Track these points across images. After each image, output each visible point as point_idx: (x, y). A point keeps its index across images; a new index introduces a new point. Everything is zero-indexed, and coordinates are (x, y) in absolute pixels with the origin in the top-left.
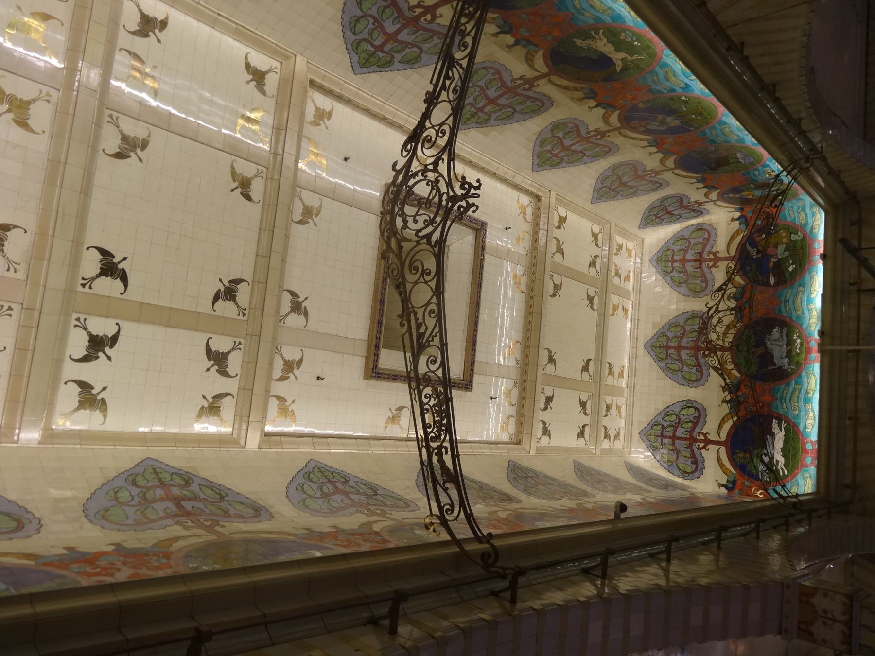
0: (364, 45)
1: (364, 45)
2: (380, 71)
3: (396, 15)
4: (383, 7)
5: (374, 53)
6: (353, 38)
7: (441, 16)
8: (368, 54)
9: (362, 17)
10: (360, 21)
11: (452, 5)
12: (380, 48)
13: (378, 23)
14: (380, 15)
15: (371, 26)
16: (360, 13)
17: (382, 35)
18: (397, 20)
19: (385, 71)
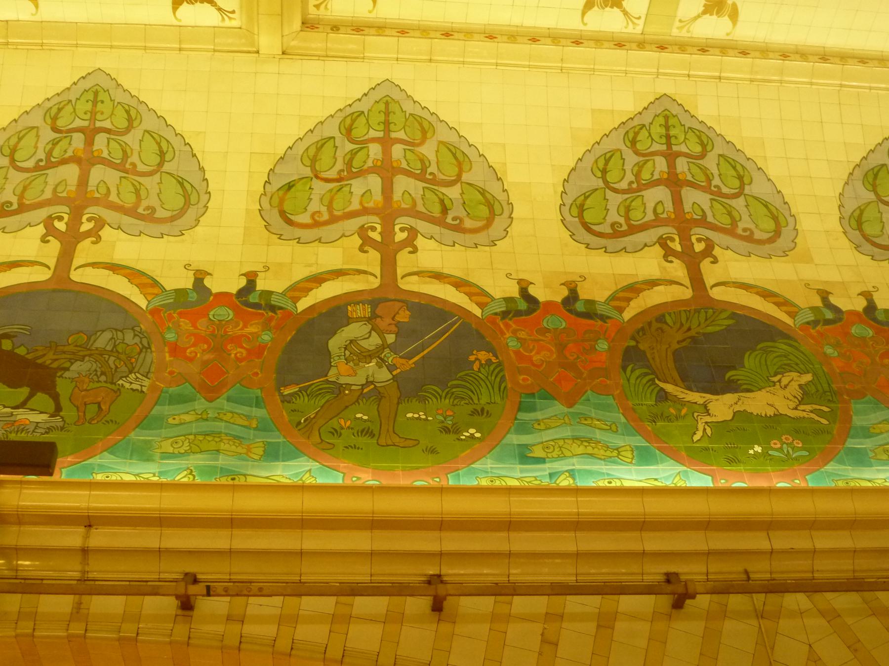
0: (121, 122)
1: (121, 122)
2: (58, 94)
3: (113, 198)
4: (143, 197)
5: (93, 119)
6: (144, 126)
7: (44, 240)
8: (102, 113)
9: (161, 164)
10: (159, 158)
11: (49, 268)
12: (90, 133)
13: (122, 167)
14: (137, 184)
15: (134, 159)
16: (167, 167)
17: (105, 154)
18: (103, 190)
19: (48, 99)
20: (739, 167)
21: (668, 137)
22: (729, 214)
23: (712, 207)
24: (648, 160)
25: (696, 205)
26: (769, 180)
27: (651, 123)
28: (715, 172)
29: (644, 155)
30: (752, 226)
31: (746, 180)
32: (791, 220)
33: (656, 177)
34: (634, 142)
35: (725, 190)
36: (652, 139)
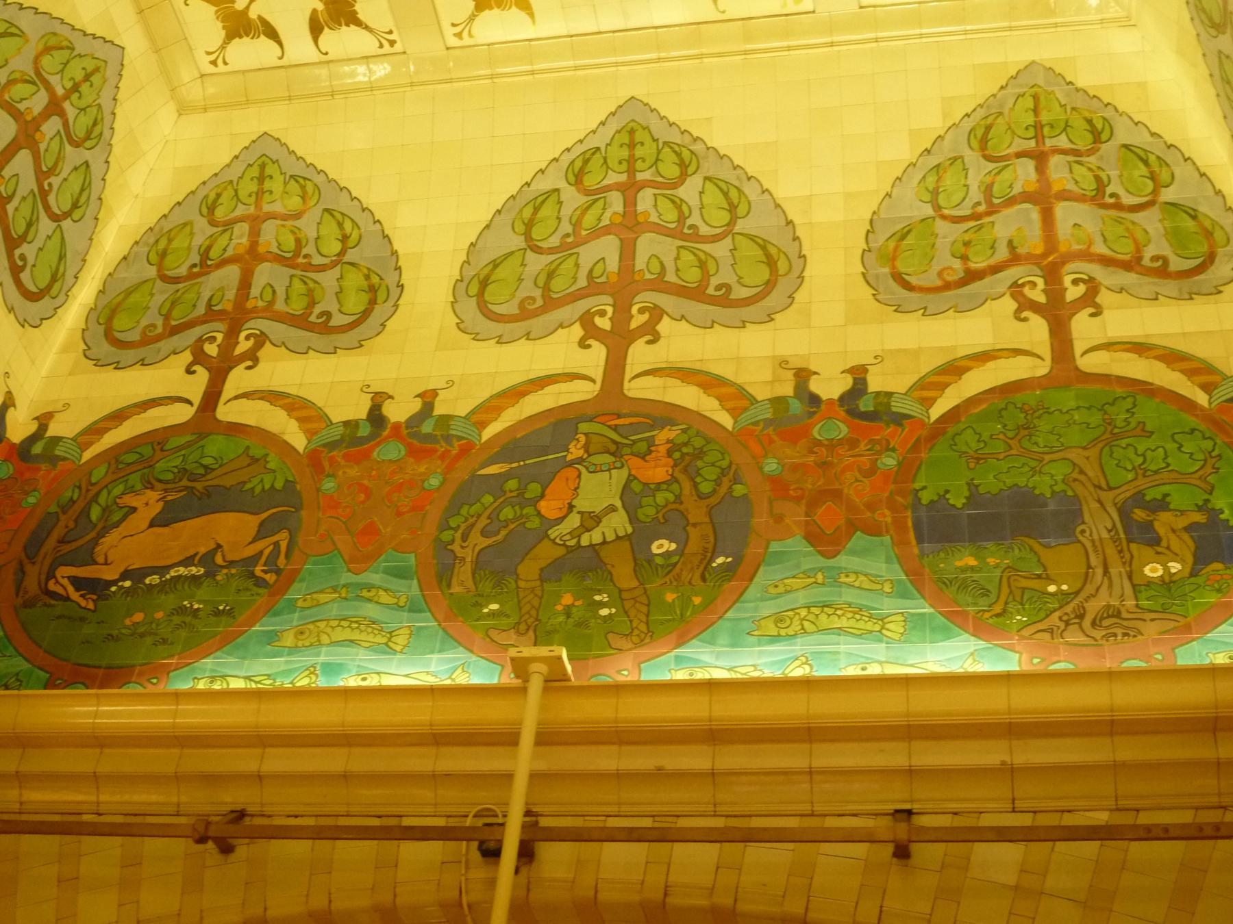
20: (85, 195)
21: (76, 88)
22: (29, 225)
23: (24, 198)
24: (34, 83)
25: (14, 180)
26: (91, 239)
27: (80, 56)
28: (64, 175)
29: (38, 73)
30: (31, 261)
31: (77, 214)
32: (62, 297)
33: (22, 107)
34: (47, 50)
35: (51, 199)
36: (62, 71)
